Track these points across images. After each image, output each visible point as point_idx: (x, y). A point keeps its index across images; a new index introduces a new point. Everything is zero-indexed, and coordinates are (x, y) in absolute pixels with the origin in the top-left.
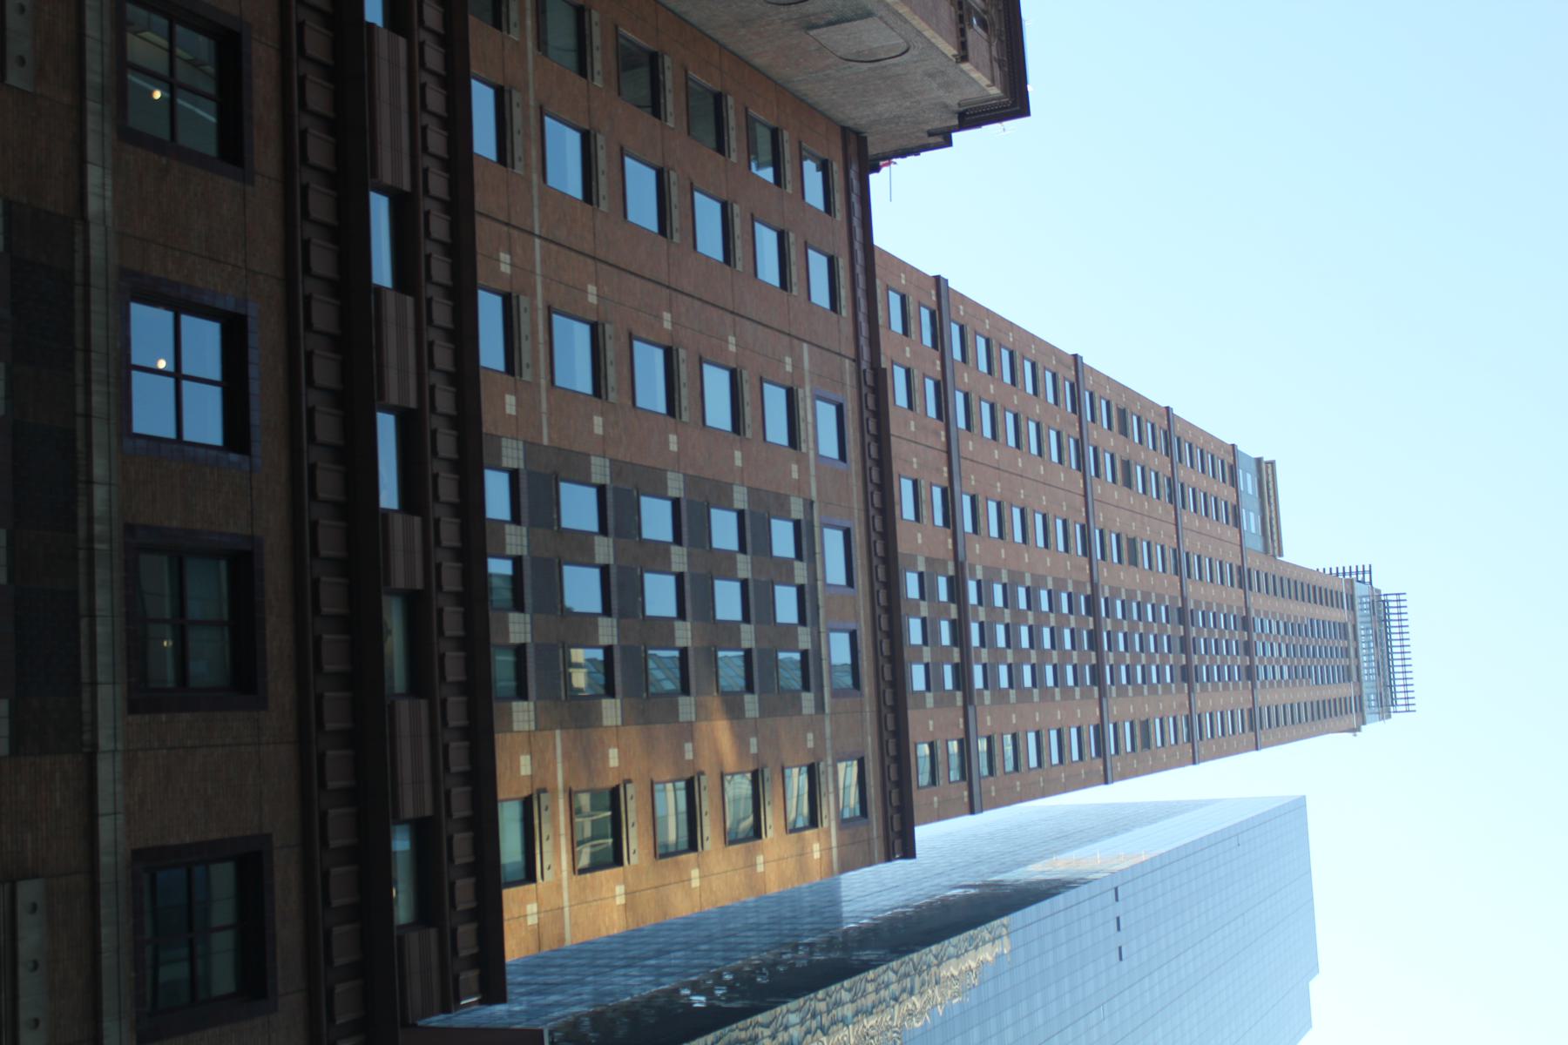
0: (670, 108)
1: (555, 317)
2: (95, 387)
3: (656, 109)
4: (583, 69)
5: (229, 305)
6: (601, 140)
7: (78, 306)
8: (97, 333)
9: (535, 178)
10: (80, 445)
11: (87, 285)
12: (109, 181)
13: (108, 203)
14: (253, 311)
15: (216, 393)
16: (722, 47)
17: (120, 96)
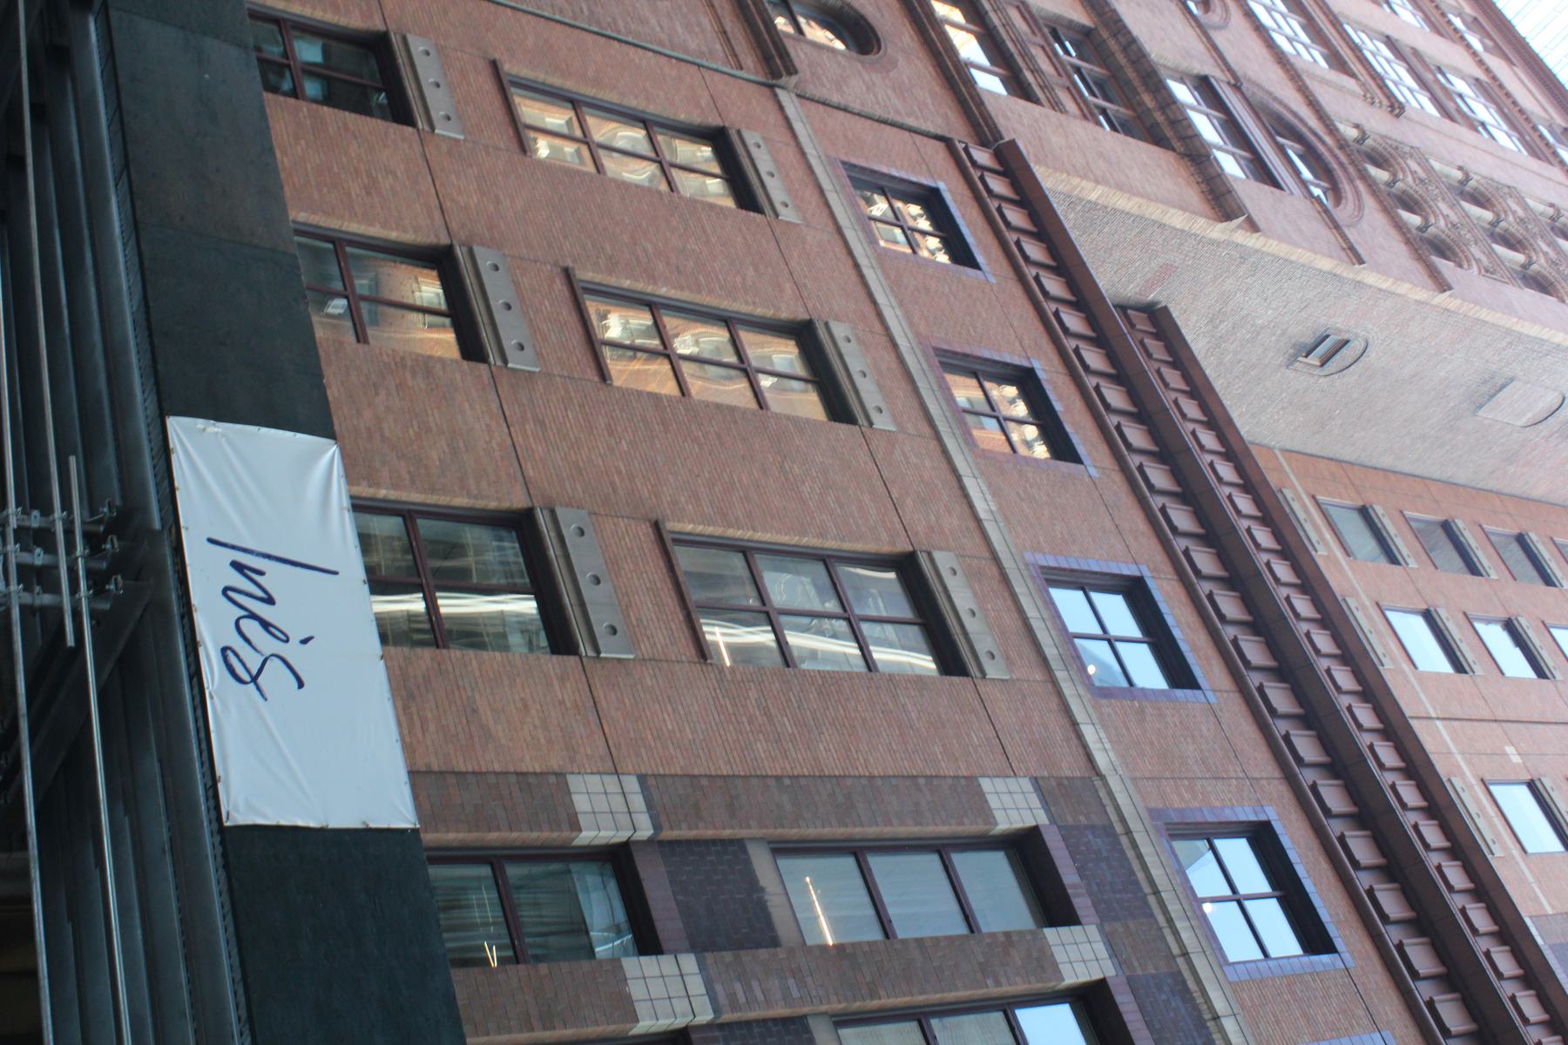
0: (1486, 563)
1: (1492, 788)
2: (1179, 925)
3: (1473, 569)
4: (1393, 559)
5: (1247, 814)
6: (1443, 613)
7: (1130, 854)
8: (1156, 873)
9: (1406, 667)
10: (1191, 985)
11: (1128, 832)
12: (1102, 735)
13: (1111, 754)
14: (1271, 814)
15: (1274, 903)
16: (1499, 494)
17: (1077, 662)
